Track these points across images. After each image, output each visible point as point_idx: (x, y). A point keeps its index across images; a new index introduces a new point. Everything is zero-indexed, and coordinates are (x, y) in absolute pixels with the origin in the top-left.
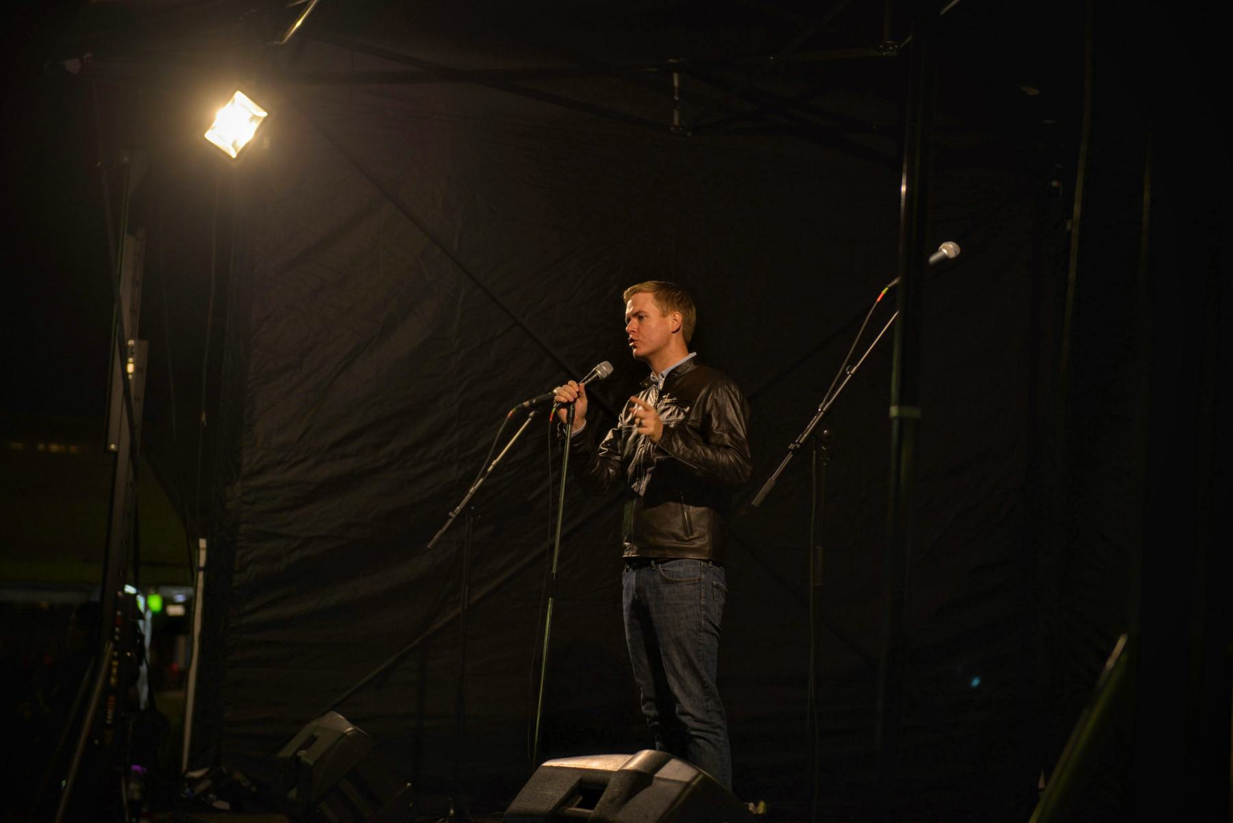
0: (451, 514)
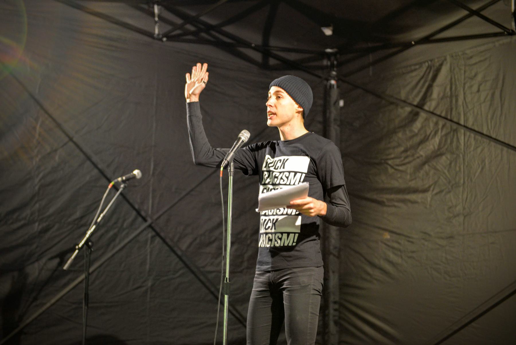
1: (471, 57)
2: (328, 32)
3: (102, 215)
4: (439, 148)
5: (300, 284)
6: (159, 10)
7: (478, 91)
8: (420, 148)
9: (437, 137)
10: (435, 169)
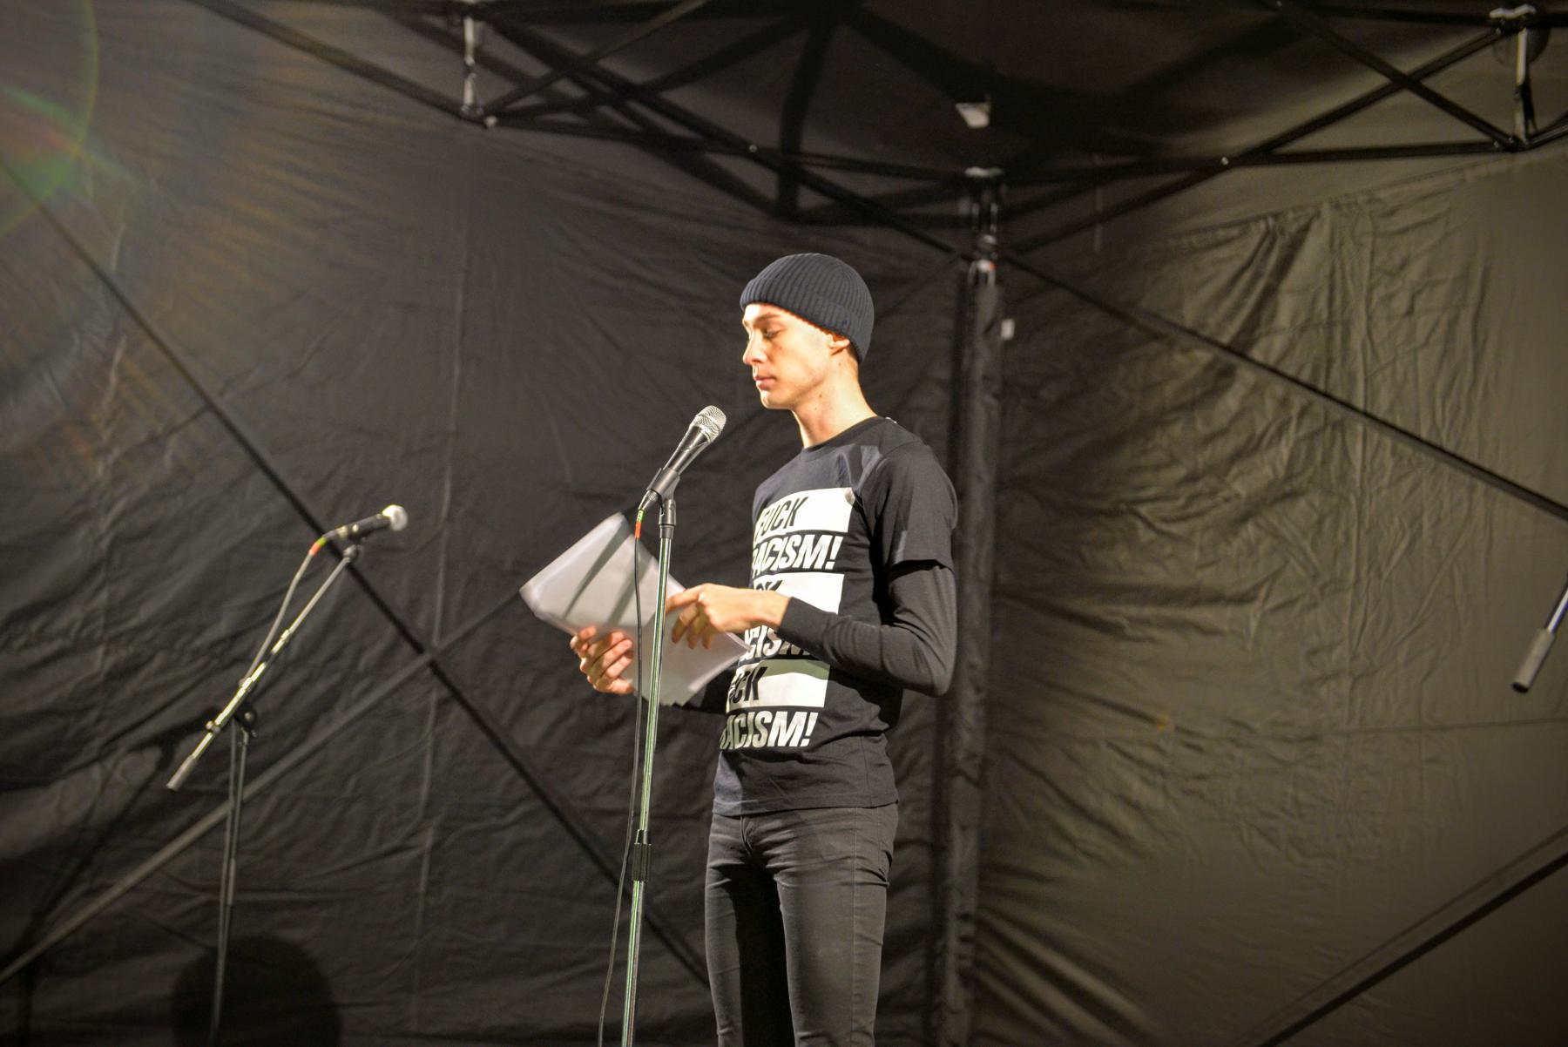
0: (209, 725)
1: (1393, 212)
2: (976, 117)
3: (285, 635)
4: (1290, 476)
5: (821, 857)
6: (481, 35)
7: (1410, 312)
8: (1234, 471)
9: (1283, 442)
10: (1275, 534)
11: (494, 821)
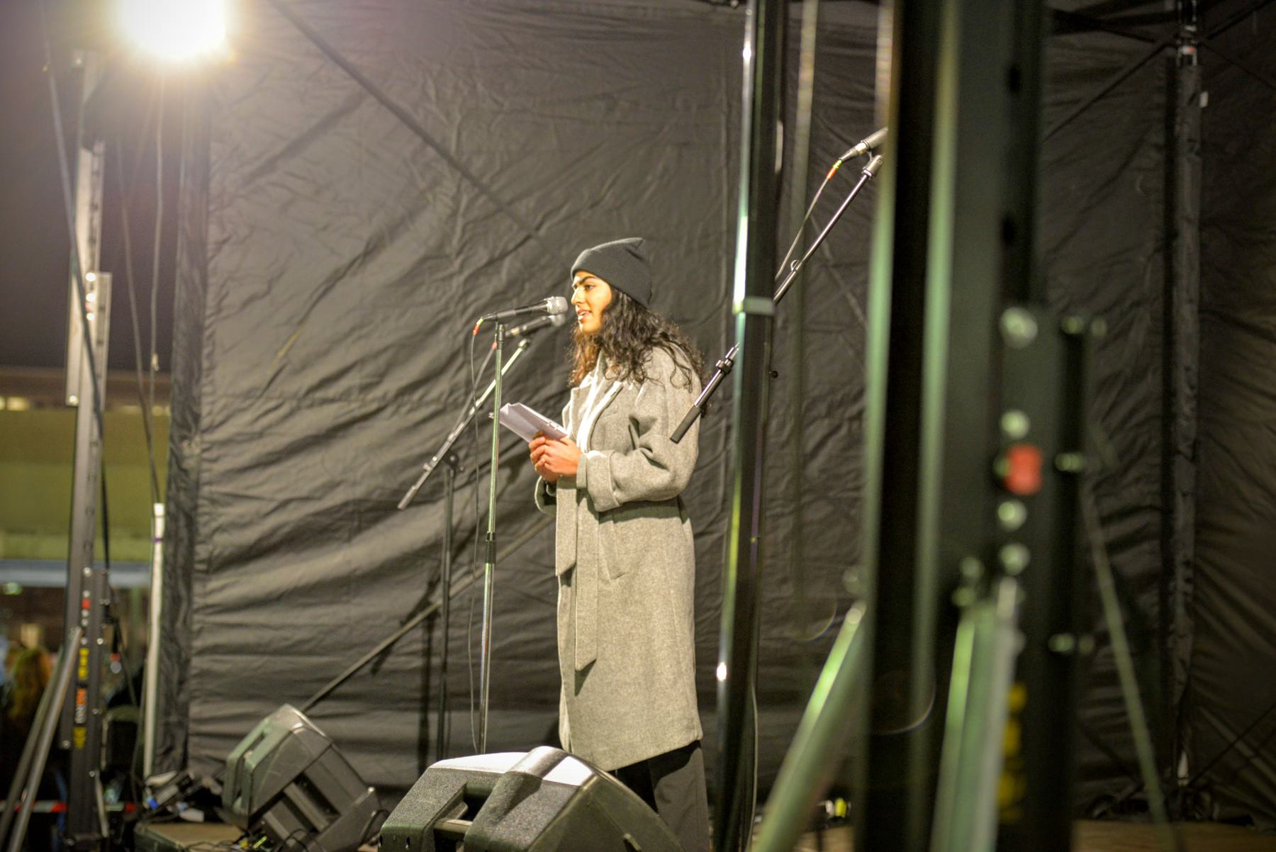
11: (779, 510)
